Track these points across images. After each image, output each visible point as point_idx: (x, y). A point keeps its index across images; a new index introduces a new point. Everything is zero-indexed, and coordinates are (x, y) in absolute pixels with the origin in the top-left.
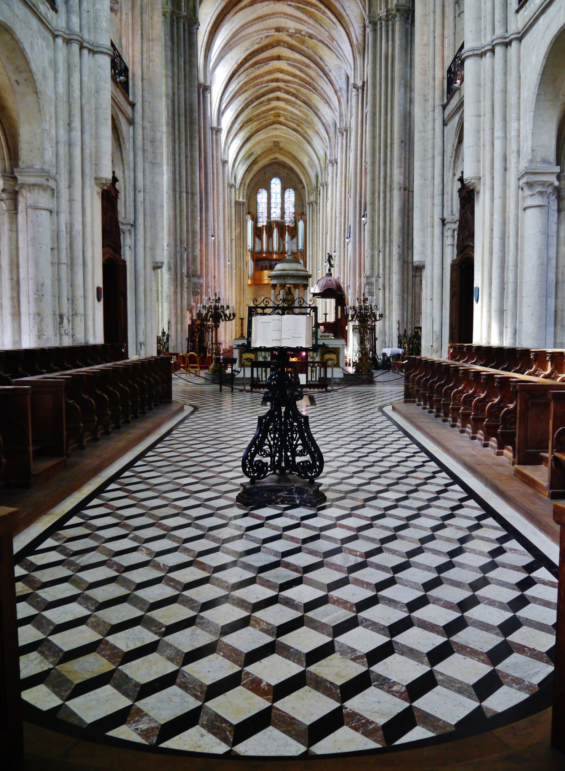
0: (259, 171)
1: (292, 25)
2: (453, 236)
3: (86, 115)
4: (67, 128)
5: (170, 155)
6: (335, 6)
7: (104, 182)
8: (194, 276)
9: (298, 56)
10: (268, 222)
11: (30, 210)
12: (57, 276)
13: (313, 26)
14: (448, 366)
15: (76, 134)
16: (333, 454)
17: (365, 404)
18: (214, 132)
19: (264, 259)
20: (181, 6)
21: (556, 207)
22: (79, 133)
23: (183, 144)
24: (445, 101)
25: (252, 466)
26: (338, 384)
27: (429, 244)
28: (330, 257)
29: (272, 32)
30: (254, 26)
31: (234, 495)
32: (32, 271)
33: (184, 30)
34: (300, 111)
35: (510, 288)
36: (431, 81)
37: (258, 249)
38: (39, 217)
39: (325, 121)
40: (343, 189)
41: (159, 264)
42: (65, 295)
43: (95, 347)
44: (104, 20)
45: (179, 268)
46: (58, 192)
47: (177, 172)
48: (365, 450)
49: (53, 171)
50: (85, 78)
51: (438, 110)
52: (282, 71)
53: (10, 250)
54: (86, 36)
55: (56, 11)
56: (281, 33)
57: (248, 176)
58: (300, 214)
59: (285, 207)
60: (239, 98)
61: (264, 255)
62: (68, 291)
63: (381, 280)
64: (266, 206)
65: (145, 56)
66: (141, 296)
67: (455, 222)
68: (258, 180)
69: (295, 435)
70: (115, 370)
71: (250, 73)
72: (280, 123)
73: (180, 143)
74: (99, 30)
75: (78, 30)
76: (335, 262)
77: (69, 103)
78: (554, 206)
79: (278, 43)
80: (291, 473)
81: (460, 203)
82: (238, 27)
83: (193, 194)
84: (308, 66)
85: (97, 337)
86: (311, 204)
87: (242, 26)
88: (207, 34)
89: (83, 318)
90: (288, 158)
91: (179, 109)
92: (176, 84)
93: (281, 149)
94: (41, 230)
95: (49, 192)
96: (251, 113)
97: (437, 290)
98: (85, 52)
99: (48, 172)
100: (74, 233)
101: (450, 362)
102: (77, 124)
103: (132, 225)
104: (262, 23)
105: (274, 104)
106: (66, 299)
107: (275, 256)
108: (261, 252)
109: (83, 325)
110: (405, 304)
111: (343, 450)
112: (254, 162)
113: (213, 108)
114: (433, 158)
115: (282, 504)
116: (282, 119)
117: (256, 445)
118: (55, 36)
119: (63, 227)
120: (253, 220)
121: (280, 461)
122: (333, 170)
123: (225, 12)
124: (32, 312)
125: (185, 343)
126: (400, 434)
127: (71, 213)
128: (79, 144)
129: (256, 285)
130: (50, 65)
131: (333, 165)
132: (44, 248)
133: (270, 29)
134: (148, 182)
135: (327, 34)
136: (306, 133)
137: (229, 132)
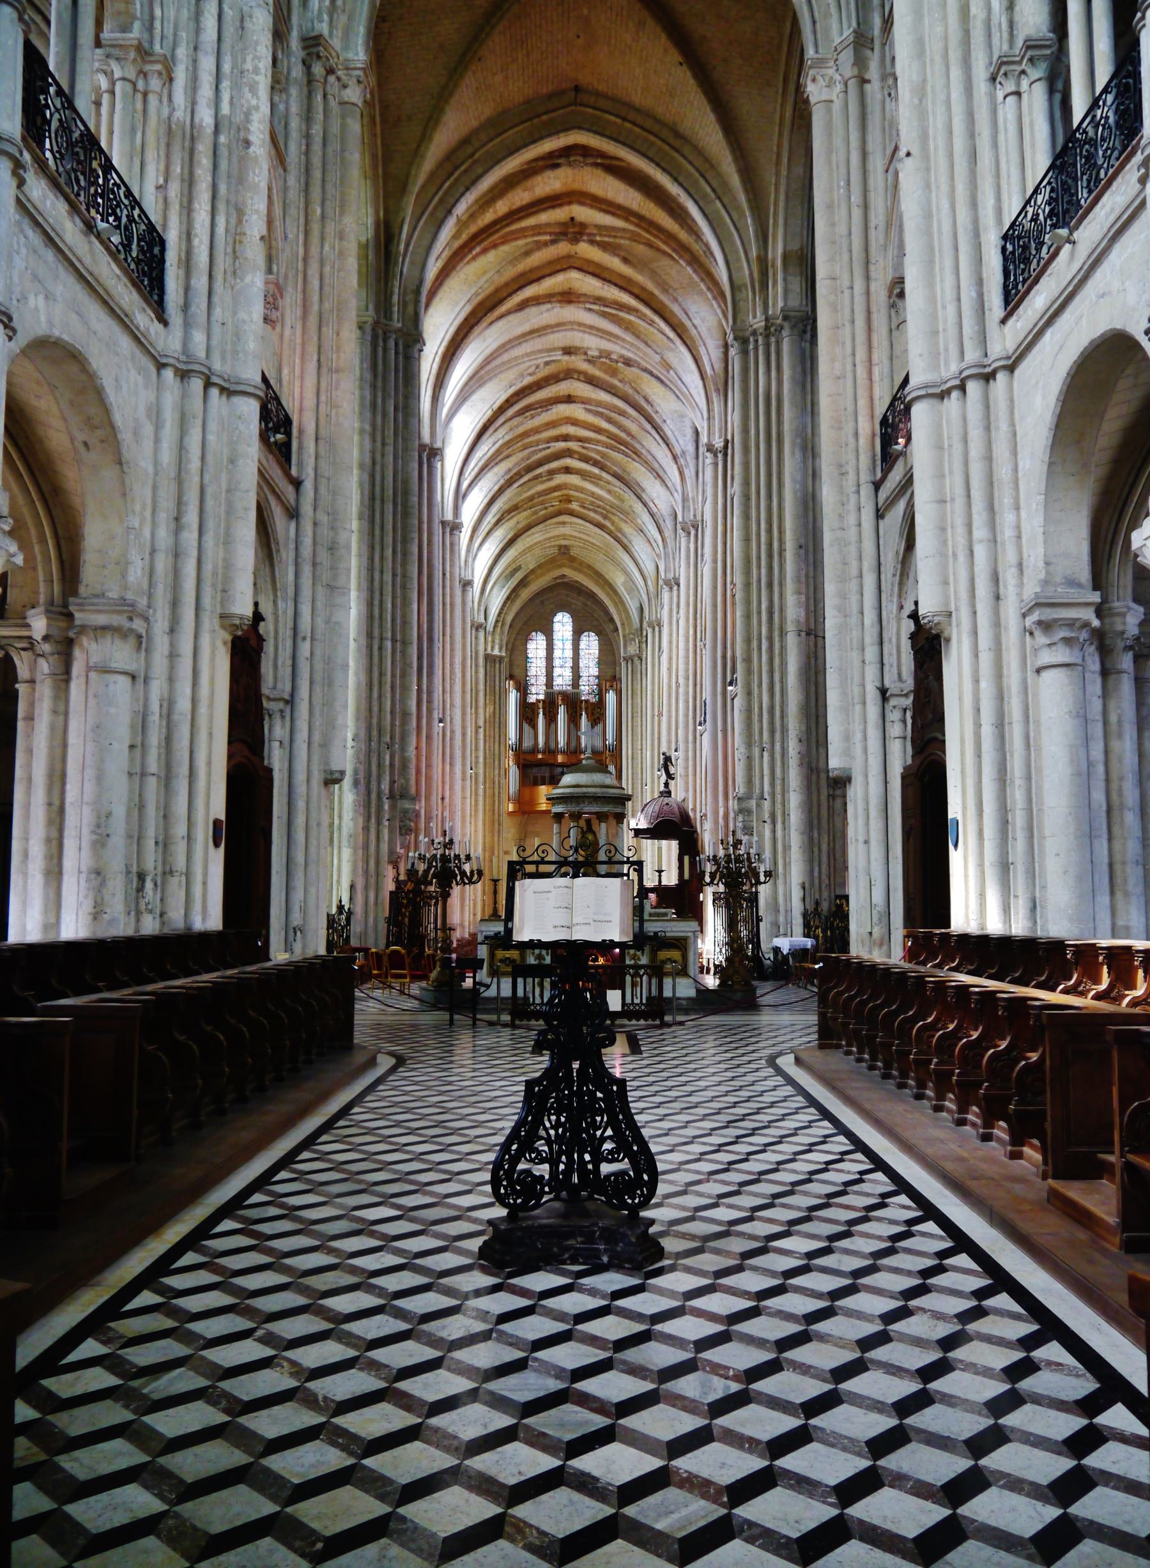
0: (531, 600)
1: (593, 343)
2: (904, 721)
3: (210, 503)
4: (173, 526)
5: (364, 572)
6: (672, 312)
7: (237, 622)
8: (402, 796)
9: (604, 396)
10: (547, 694)
11: (93, 675)
12: (136, 798)
13: (632, 344)
14: (903, 975)
15: (190, 537)
16: (677, 1157)
17: (740, 1051)
19: (540, 764)
20: (391, 313)
21: (1097, 667)
22: (196, 534)
23: (389, 553)
24: (879, 475)
25: (511, 1184)
26: (686, 1012)
27: (858, 736)
28: (668, 760)
29: (558, 356)
30: (524, 346)
31: (475, 1244)
32: (89, 787)
33: (396, 353)
34: (609, 492)
35: (1018, 820)
36: (851, 440)
37: (527, 744)
38: (111, 687)
39: (655, 510)
40: (691, 632)
41: (337, 776)
42: (151, 833)
43: (205, 936)
44: (252, 338)
45: (374, 783)
46: (150, 639)
47: (376, 603)
48: (742, 1148)
49: (143, 602)
50: (211, 438)
51: (866, 490)
52: (575, 422)
53: (51, 748)
54: (217, 366)
55: (163, 321)
56: (573, 358)
58: (609, 678)
60: (496, 470)
62: (157, 828)
63: (767, 805)
65: (323, 398)
66: (300, 836)
67: (906, 695)
68: (529, 616)
69: (598, 1119)
70: (242, 983)
71: (517, 426)
72: (572, 513)
73: (382, 550)
74: (241, 355)
75: (203, 355)
76: (677, 769)
77: (180, 481)
78: (1094, 665)
79: (568, 374)
80: (590, 1198)
81: (915, 659)
82: (494, 346)
83: (405, 643)
84: (622, 413)
85: (209, 915)
86: (629, 659)
87: (503, 345)
88: (438, 359)
89: (183, 878)
90: (587, 575)
91: (383, 490)
92: (379, 444)
93: (573, 559)
94: (112, 710)
95: (132, 641)
96: (519, 494)
97: (876, 825)
98: (214, 392)
99: (132, 605)
100: (175, 717)
101: (907, 966)
102: (191, 517)
103: (287, 702)
104: (538, 340)
105: (560, 479)
106: (152, 843)
107: (560, 759)
108: (535, 750)
109: (183, 894)
110: (816, 850)
111: (697, 1148)
112: (523, 583)
113: (446, 487)
114: (861, 576)
115: (573, 1264)
116: (574, 506)
117: (522, 1138)
118: (161, 366)
119: (155, 707)
120: (518, 690)
121: (568, 1172)
122: (671, 598)
123: (472, 321)
124: (84, 868)
125: (383, 926)
126: (812, 1114)
127: (171, 680)
128: (195, 553)
129: (524, 813)
130: (149, 416)
132: (116, 745)
133: (554, 349)
134: (320, 621)
135: (657, 358)
136: (620, 530)
137: (474, 530)
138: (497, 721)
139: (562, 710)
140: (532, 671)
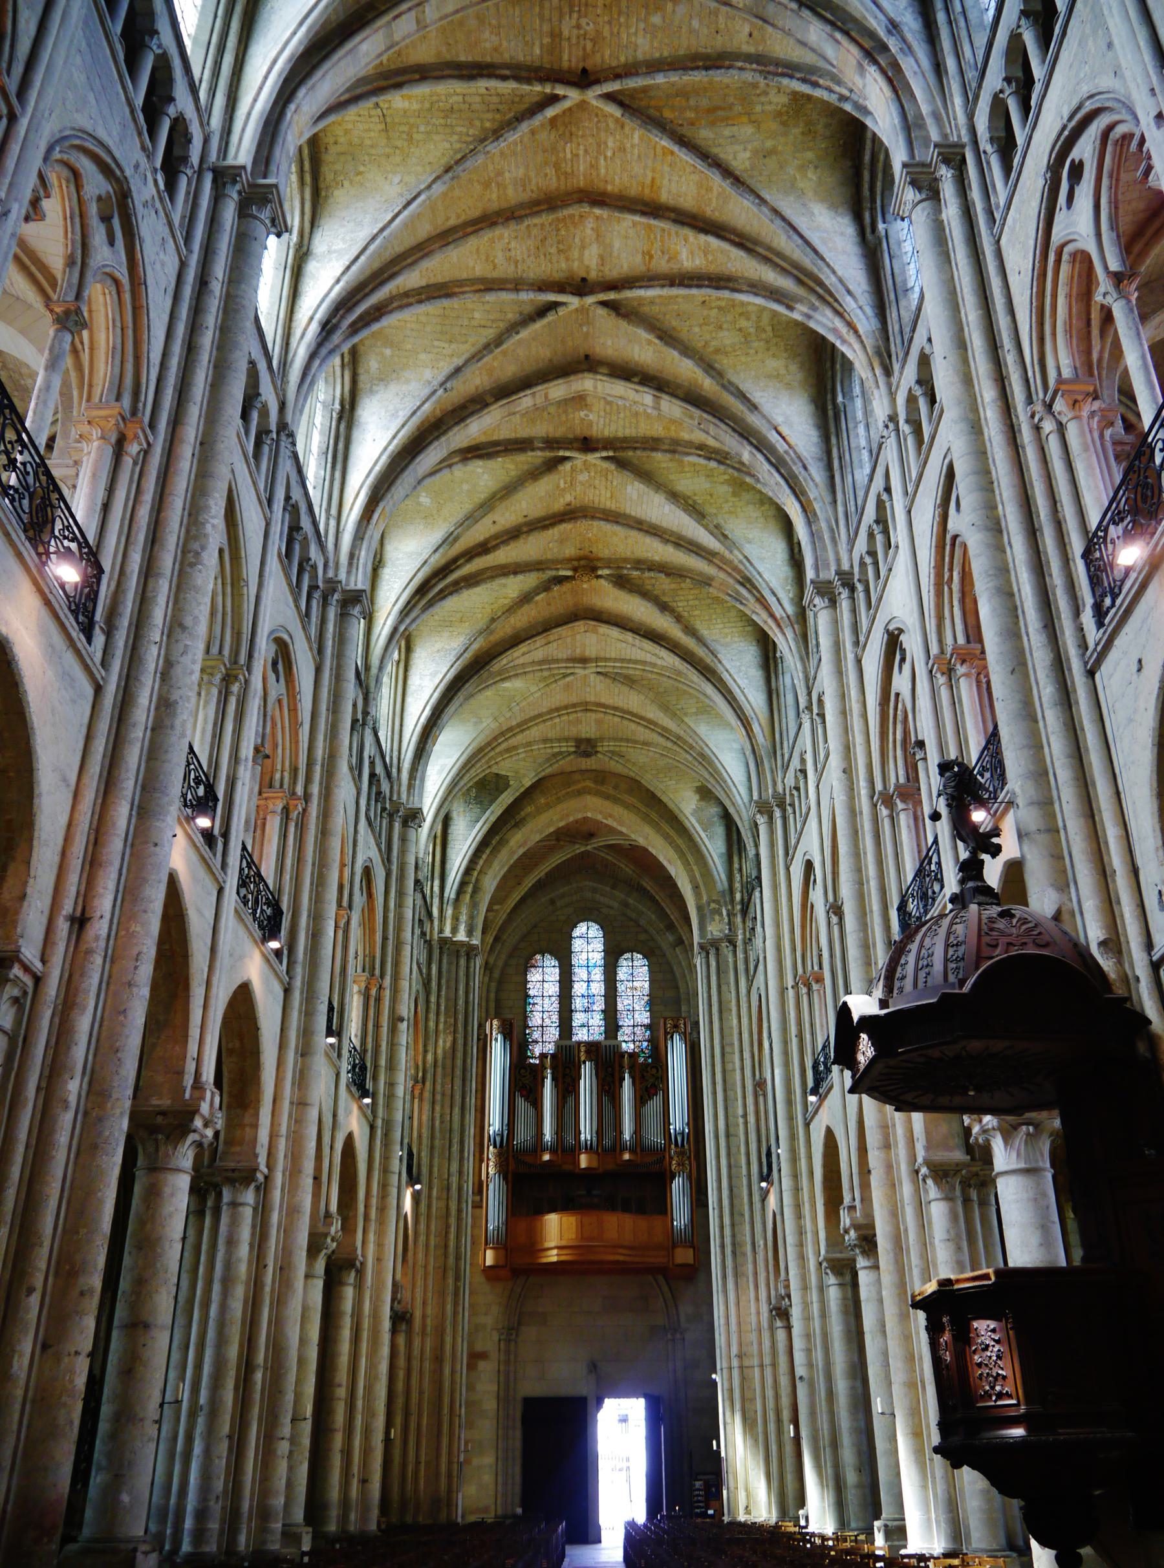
10: (558, 1046)
18: (233, 195)
37: (523, 1135)
40: (987, 393)
58: (671, 1006)
59: (620, 1007)
61: (546, 1157)
64: (556, 1005)
120: (507, 1032)
131: (833, 603)
139: (587, 1071)
140: (535, 1020)
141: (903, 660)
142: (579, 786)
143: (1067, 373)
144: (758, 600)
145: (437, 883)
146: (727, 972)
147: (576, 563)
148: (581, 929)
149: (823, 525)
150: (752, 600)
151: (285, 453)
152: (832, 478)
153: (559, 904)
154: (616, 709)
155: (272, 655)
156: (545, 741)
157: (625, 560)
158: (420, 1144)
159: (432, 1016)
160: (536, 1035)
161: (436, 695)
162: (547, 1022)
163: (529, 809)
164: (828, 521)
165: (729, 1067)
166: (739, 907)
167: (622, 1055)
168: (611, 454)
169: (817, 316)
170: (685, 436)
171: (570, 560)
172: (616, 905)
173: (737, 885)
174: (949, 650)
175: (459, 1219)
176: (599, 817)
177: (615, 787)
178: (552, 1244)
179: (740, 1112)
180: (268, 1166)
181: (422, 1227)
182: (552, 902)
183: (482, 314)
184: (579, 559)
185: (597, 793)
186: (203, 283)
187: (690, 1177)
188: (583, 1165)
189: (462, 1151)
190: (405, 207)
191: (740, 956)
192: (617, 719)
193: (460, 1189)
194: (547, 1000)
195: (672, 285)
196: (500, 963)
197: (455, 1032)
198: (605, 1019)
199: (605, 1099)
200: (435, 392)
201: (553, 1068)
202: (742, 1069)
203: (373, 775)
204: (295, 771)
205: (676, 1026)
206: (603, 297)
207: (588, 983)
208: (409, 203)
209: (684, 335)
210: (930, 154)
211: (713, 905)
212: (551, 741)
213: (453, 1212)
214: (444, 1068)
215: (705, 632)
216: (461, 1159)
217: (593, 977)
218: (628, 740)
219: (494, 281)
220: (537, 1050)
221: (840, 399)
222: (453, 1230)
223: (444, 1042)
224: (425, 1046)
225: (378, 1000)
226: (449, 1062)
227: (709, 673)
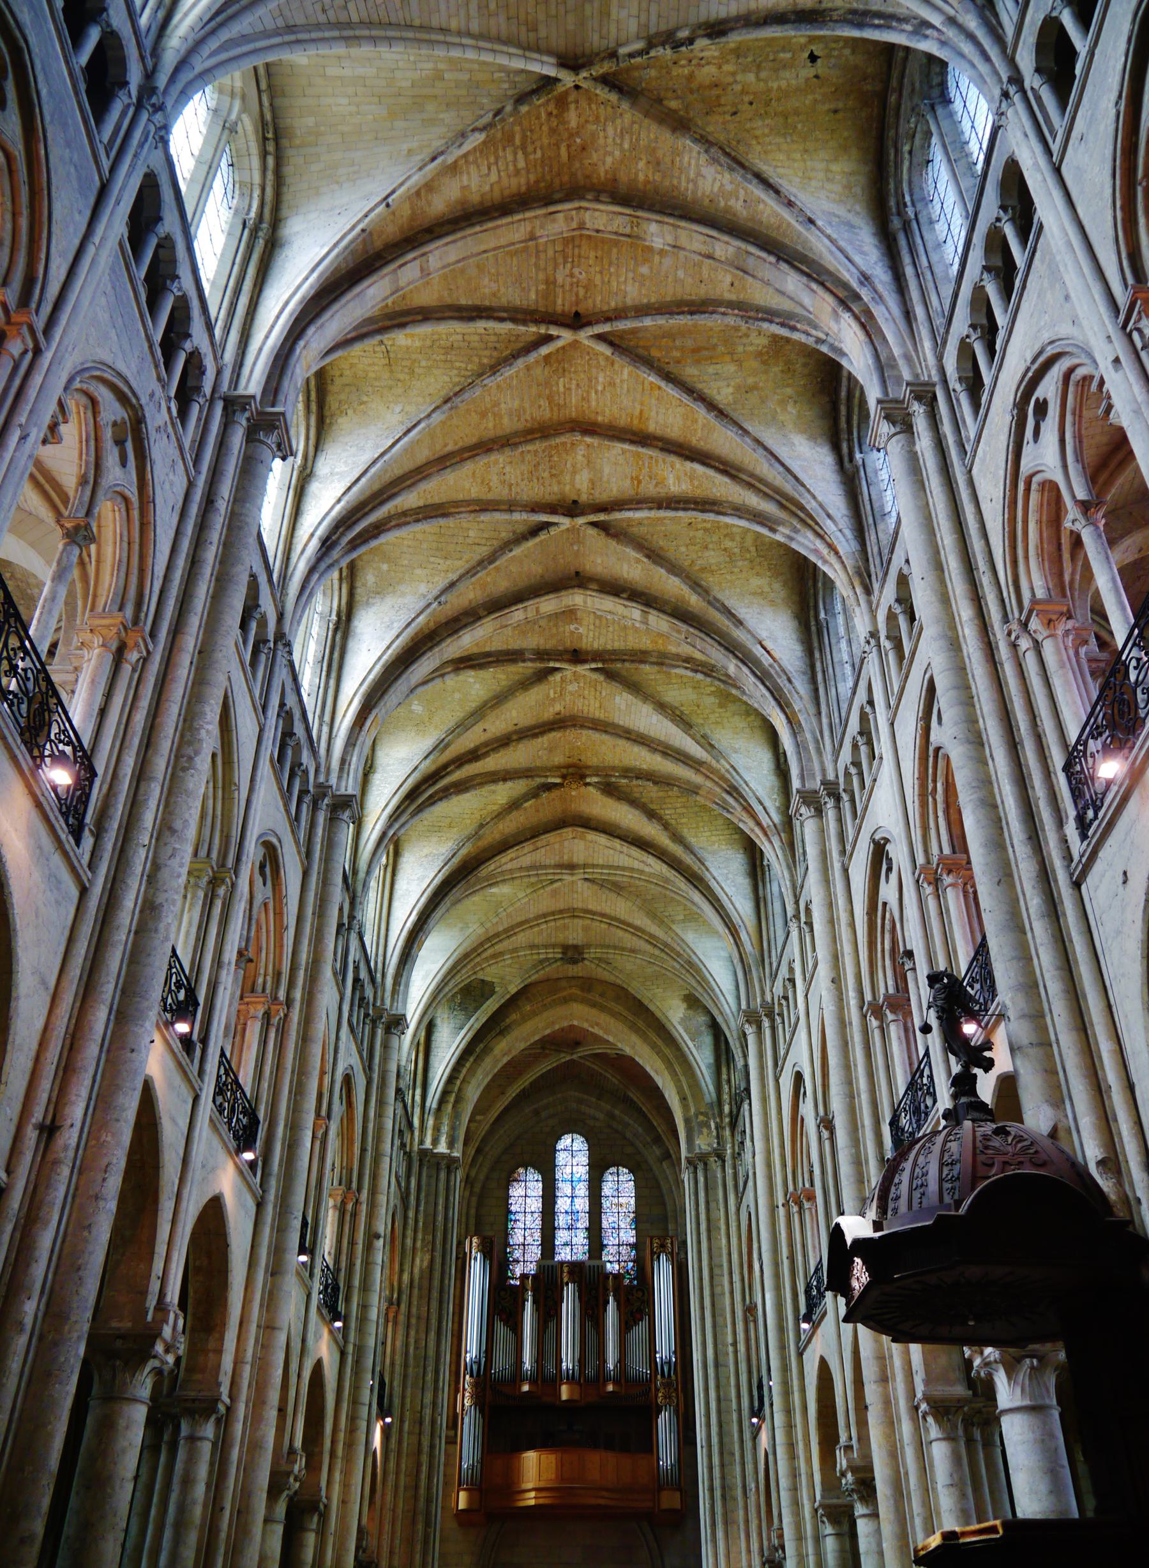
18: (242, 421)
37: (501, 1363)
40: (965, 612)
57: (472, 1071)
58: (658, 1223)
59: (605, 1224)
64: (539, 1222)
120: (487, 1251)
122: (822, 832)
131: (819, 812)
138: (438, 1296)
140: (517, 1237)
141: (889, 869)
142: (565, 993)
143: (1040, 594)
144: (745, 808)
145: (418, 1092)
146: (715, 1188)
147: (564, 771)
148: (565, 1141)
149: (808, 736)
150: (739, 809)
151: (281, 660)
152: (816, 690)
153: (544, 1114)
154: (603, 915)
155: (260, 857)
156: (532, 947)
157: (614, 768)
158: (392, 1373)
159: (410, 1233)
160: (517, 1254)
161: (423, 900)
162: (529, 1240)
163: (514, 1017)
164: (813, 733)
165: (718, 1290)
166: (727, 1120)
167: (607, 1276)
168: (600, 665)
169: (799, 538)
170: (673, 649)
171: (559, 767)
172: (601, 1116)
173: (726, 1097)
174: (935, 860)
175: (431, 1456)
176: (585, 1025)
177: (602, 995)
178: (530, 1486)
179: (730, 1340)
180: (230, 1397)
181: (392, 1465)
182: (537, 1113)
183: (477, 533)
184: (568, 767)
185: (584, 1001)
186: (209, 501)
187: (677, 1412)
188: (564, 1396)
189: (436, 1381)
190: (405, 434)
191: (729, 1171)
192: (603, 926)
193: (433, 1422)
194: (529, 1216)
195: (659, 508)
196: (482, 1177)
197: (433, 1250)
198: (589, 1238)
199: (588, 1324)
200: (429, 605)
201: (534, 1290)
202: (732, 1292)
203: (356, 980)
204: (278, 975)
205: (663, 1246)
206: (593, 518)
207: (572, 1199)
208: (409, 431)
209: (671, 555)
210: (903, 392)
211: (701, 1118)
212: (537, 947)
213: (426, 1449)
214: (420, 1289)
215: (692, 840)
216: (436, 1389)
217: (577, 1192)
218: (615, 947)
219: (489, 502)
220: (518, 1270)
221: (822, 615)
222: (424, 1468)
223: (421, 1261)
224: (401, 1265)
225: (354, 1215)
226: (426, 1284)
227: (696, 880)
